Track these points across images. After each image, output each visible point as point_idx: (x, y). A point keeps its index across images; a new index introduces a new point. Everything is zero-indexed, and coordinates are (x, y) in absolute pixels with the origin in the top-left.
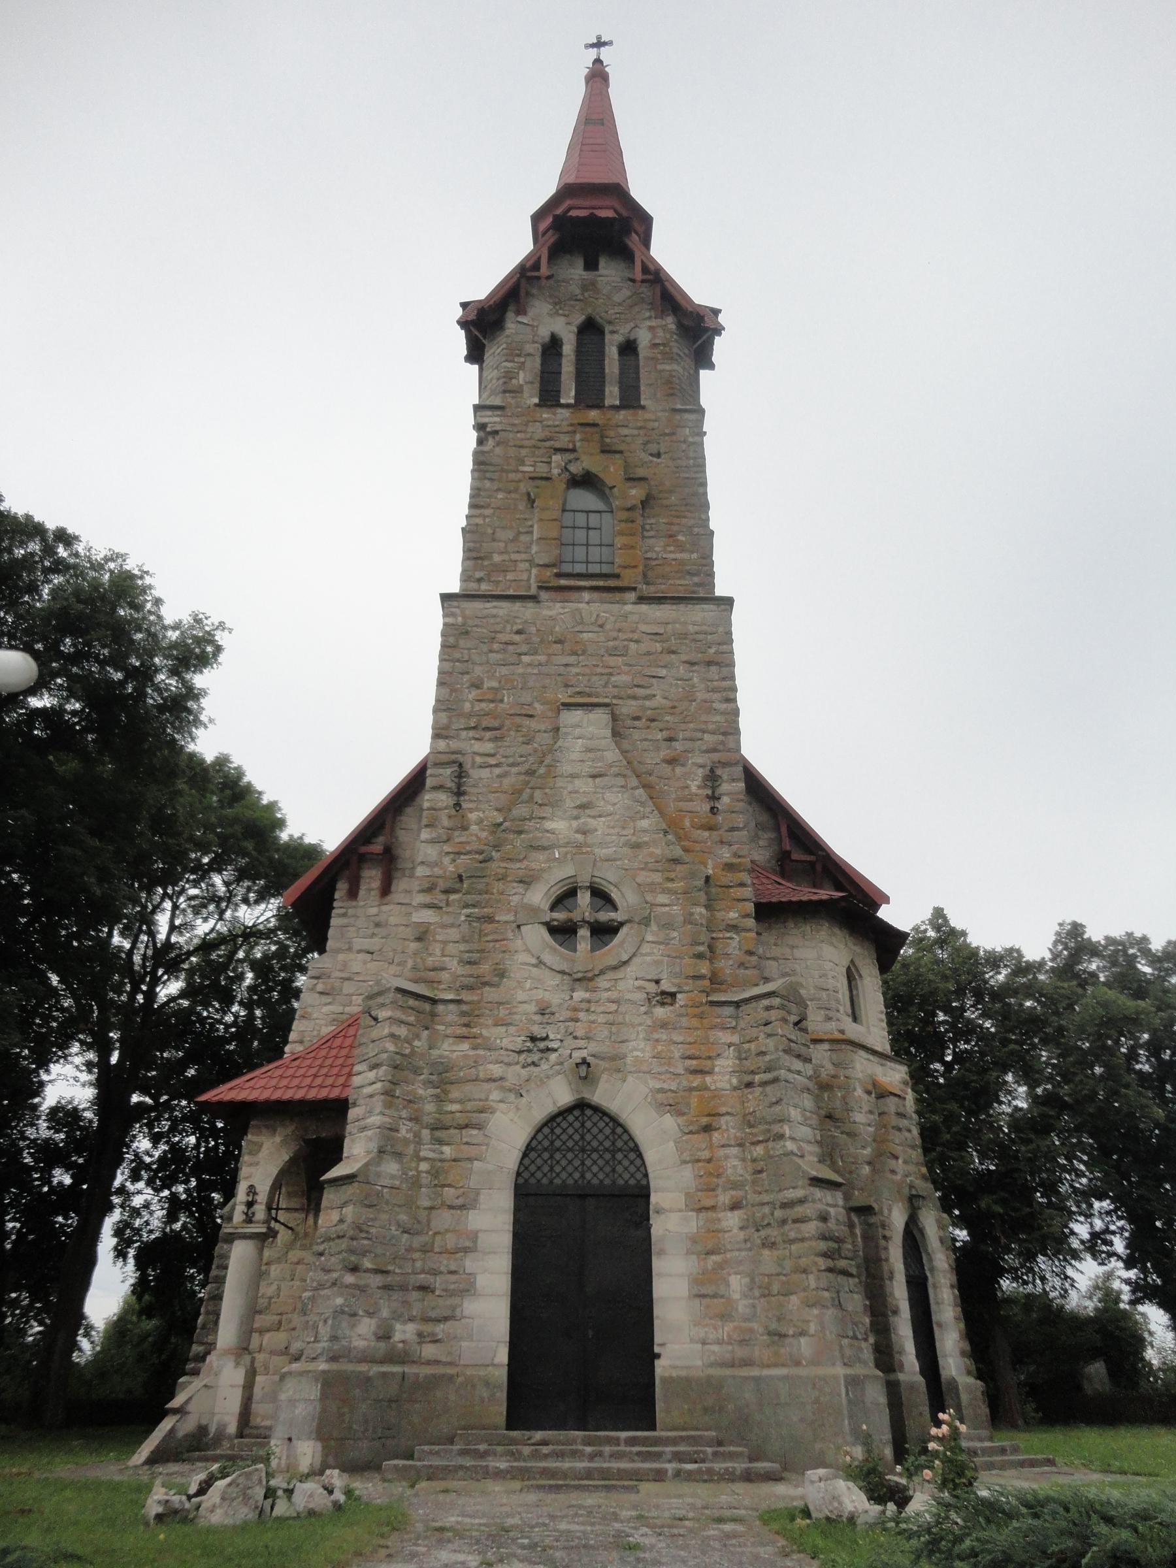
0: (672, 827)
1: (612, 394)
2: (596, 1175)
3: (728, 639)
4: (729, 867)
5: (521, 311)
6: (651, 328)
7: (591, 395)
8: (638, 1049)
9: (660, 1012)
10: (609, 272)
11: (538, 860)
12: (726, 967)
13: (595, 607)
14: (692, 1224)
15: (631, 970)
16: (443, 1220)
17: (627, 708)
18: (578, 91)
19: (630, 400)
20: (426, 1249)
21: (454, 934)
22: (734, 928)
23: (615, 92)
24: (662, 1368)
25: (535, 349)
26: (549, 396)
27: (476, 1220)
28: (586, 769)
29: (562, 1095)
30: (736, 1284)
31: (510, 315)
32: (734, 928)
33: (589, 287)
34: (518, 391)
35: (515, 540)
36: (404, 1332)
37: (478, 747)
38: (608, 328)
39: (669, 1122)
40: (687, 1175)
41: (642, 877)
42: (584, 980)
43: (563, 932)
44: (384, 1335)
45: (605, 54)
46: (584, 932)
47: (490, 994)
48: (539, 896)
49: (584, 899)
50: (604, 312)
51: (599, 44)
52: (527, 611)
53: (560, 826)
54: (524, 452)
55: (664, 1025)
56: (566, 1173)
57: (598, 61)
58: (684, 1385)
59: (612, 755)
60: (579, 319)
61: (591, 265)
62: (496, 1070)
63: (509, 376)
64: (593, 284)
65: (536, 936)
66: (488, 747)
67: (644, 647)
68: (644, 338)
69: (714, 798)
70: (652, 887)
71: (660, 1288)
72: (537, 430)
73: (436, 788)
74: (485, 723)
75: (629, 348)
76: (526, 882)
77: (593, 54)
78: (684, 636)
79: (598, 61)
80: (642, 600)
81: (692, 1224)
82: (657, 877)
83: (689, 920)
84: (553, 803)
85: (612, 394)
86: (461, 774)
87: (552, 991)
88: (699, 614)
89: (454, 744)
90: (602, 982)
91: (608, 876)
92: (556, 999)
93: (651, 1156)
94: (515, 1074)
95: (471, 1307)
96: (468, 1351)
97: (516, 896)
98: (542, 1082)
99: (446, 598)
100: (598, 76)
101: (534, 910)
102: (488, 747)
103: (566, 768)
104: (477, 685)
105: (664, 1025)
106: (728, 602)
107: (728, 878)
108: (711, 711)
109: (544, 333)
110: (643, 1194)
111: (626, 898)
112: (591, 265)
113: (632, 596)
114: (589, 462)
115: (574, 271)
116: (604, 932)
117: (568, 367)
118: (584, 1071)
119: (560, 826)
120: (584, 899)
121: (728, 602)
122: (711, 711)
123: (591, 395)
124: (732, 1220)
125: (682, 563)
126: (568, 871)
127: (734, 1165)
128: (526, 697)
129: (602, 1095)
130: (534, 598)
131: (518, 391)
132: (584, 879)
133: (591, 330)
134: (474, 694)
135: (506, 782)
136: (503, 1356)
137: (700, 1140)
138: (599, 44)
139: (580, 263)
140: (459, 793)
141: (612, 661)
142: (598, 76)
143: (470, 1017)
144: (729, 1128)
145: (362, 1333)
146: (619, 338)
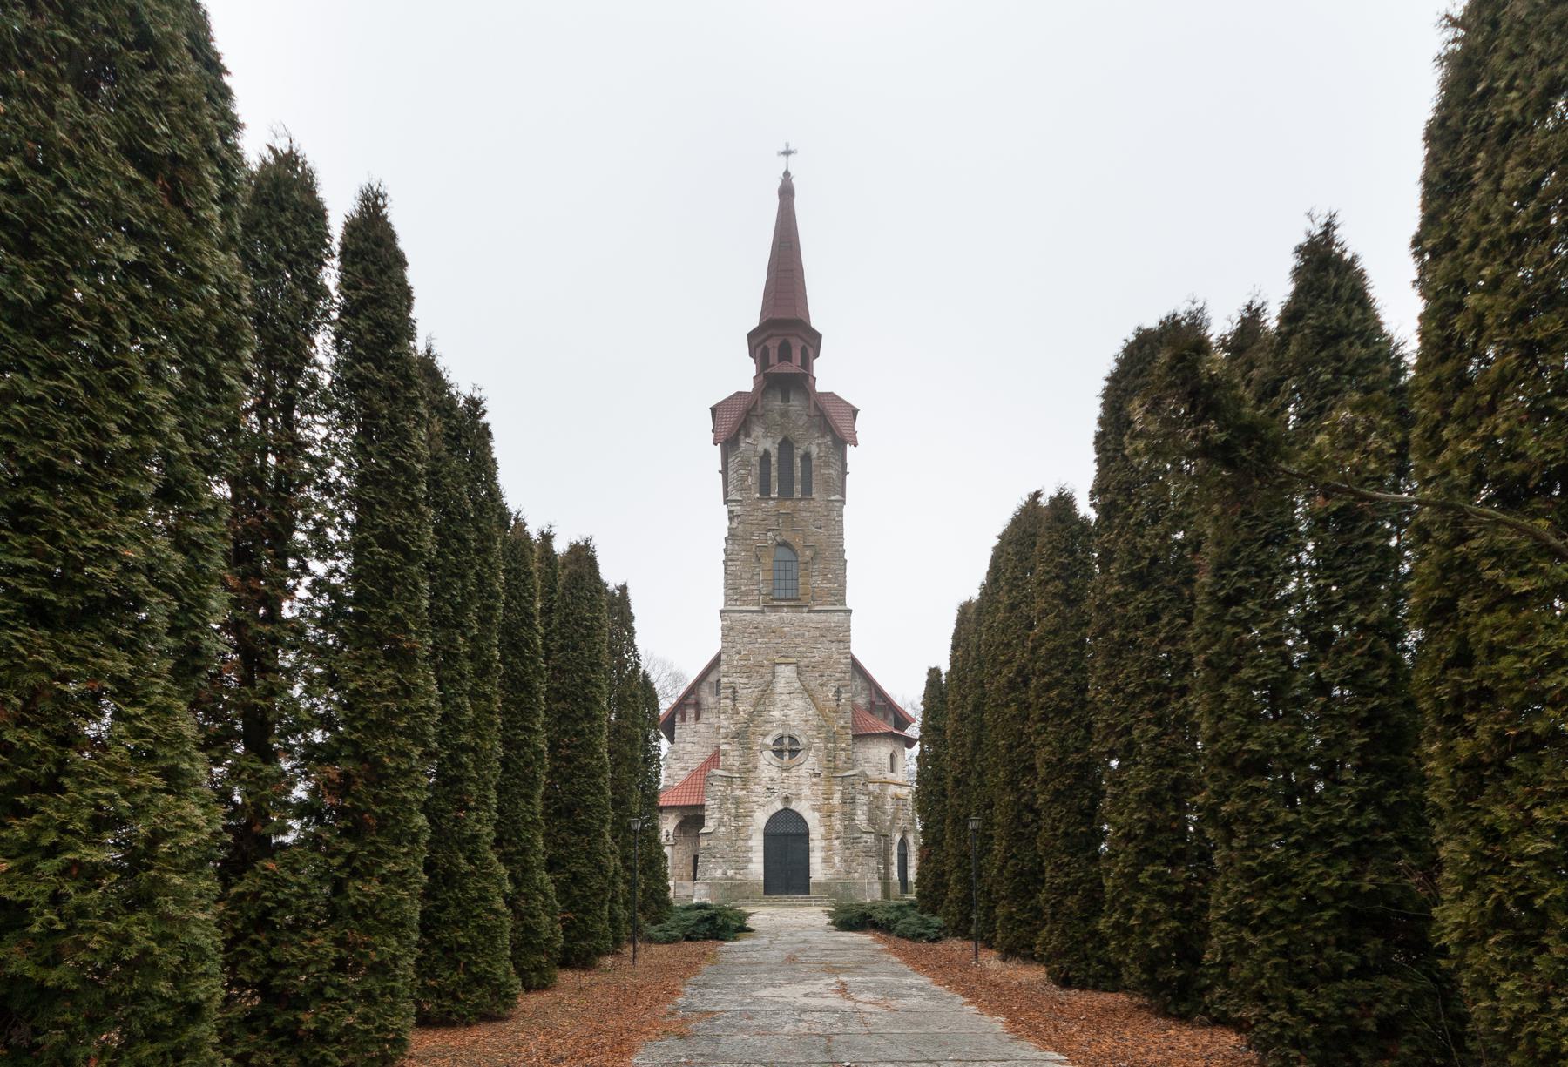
0: (821, 711)
1: (798, 495)
2: (792, 830)
3: (848, 630)
4: (843, 727)
5: (748, 435)
6: (819, 445)
7: (786, 493)
8: (806, 791)
9: (814, 780)
10: (796, 404)
11: (768, 727)
12: (840, 763)
13: (790, 615)
14: (824, 843)
15: (804, 766)
16: (741, 843)
17: (805, 662)
18: (774, 203)
19: (807, 492)
20: (735, 851)
21: (736, 753)
22: (843, 750)
23: (798, 203)
24: (811, 881)
25: (755, 460)
26: (765, 490)
27: (751, 843)
28: (786, 690)
29: (779, 806)
30: (837, 859)
31: (742, 437)
32: (843, 750)
33: (785, 414)
34: (748, 489)
35: (751, 578)
36: (730, 872)
37: (741, 680)
38: (796, 445)
39: (817, 814)
40: (822, 830)
41: (809, 733)
42: (787, 770)
43: (779, 753)
44: (725, 873)
45: (794, 164)
46: (787, 753)
47: (752, 774)
48: (769, 741)
49: (786, 741)
50: (796, 434)
51: (787, 153)
52: (759, 617)
53: (776, 714)
54: (754, 528)
55: (816, 784)
56: (781, 830)
57: (787, 174)
58: (818, 885)
59: (797, 685)
60: (779, 439)
61: (786, 399)
62: (755, 799)
63: (743, 479)
64: (787, 412)
65: (768, 754)
66: (746, 680)
67: (811, 634)
68: (814, 450)
69: (838, 700)
70: (812, 736)
71: (812, 860)
72: (759, 515)
73: (726, 698)
74: (744, 670)
75: (807, 457)
76: (764, 735)
77: (780, 165)
78: (828, 629)
79: (787, 174)
80: (810, 611)
81: (824, 843)
82: (814, 733)
83: (826, 748)
84: (773, 704)
85: (798, 495)
86: (735, 692)
87: (775, 773)
88: (836, 617)
89: (731, 679)
90: (793, 770)
91: (796, 733)
92: (776, 776)
93: (810, 824)
94: (762, 800)
95: (750, 866)
96: (751, 877)
97: (760, 740)
98: (772, 802)
99: (722, 612)
100: (786, 192)
101: (767, 746)
102: (746, 680)
103: (778, 690)
104: (738, 653)
105: (816, 784)
106: (850, 611)
107: (843, 731)
108: (840, 663)
109: (760, 449)
110: (807, 834)
111: (803, 740)
112: (786, 399)
113: (806, 609)
114: (786, 536)
115: (776, 404)
116: (794, 753)
117: (774, 473)
118: (787, 799)
119: (776, 714)
120: (786, 741)
121: (850, 611)
122: (840, 663)
123: (786, 493)
124: (836, 842)
125: (830, 589)
126: (780, 731)
127: (838, 826)
128: (760, 658)
129: (793, 806)
130: (762, 612)
131: (748, 489)
132: (786, 734)
133: (786, 446)
134: (737, 657)
135: (754, 695)
136: (762, 878)
137: (827, 820)
138: (787, 153)
139: (779, 397)
140: (734, 700)
141: (797, 641)
142: (786, 192)
143: (745, 782)
144: (837, 815)
145: (719, 873)
146: (800, 452)
